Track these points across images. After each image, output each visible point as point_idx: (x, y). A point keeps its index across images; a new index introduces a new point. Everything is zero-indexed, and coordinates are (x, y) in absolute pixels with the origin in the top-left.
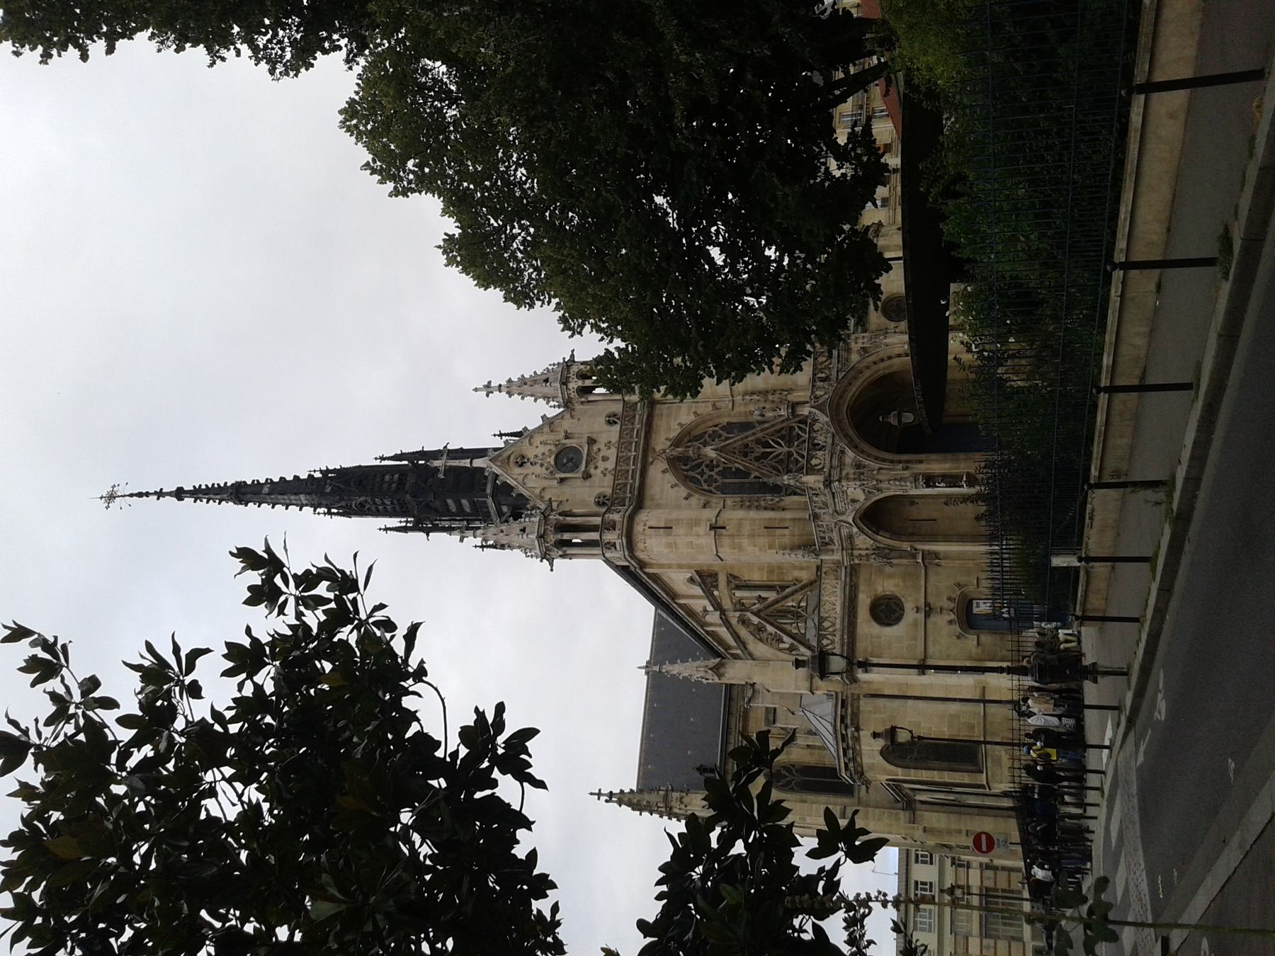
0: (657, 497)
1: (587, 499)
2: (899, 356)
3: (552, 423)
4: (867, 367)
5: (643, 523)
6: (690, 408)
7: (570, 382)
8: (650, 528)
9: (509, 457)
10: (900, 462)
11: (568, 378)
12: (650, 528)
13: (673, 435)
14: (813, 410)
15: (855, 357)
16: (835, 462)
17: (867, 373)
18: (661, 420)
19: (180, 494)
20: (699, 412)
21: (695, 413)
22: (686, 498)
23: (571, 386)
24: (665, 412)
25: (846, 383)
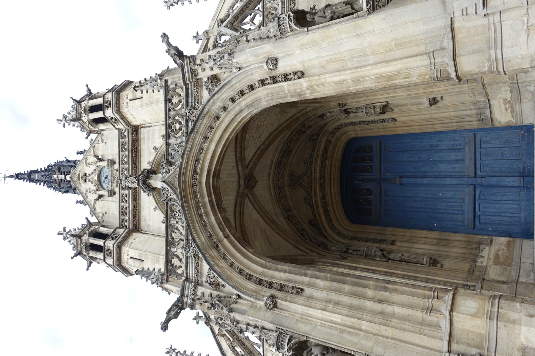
0: (147, 218)
1: (115, 213)
2: (263, 82)
3: (94, 147)
4: (225, 109)
5: (126, 254)
7: (82, 117)
8: (131, 258)
9: (79, 175)
10: (271, 285)
11: (81, 113)
12: (131, 258)
13: (151, 159)
14: (165, 185)
15: (205, 94)
17: (226, 118)
18: (144, 143)
19: (18, 176)
23: (83, 119)
24: (146, 135)
25: (199, 138)
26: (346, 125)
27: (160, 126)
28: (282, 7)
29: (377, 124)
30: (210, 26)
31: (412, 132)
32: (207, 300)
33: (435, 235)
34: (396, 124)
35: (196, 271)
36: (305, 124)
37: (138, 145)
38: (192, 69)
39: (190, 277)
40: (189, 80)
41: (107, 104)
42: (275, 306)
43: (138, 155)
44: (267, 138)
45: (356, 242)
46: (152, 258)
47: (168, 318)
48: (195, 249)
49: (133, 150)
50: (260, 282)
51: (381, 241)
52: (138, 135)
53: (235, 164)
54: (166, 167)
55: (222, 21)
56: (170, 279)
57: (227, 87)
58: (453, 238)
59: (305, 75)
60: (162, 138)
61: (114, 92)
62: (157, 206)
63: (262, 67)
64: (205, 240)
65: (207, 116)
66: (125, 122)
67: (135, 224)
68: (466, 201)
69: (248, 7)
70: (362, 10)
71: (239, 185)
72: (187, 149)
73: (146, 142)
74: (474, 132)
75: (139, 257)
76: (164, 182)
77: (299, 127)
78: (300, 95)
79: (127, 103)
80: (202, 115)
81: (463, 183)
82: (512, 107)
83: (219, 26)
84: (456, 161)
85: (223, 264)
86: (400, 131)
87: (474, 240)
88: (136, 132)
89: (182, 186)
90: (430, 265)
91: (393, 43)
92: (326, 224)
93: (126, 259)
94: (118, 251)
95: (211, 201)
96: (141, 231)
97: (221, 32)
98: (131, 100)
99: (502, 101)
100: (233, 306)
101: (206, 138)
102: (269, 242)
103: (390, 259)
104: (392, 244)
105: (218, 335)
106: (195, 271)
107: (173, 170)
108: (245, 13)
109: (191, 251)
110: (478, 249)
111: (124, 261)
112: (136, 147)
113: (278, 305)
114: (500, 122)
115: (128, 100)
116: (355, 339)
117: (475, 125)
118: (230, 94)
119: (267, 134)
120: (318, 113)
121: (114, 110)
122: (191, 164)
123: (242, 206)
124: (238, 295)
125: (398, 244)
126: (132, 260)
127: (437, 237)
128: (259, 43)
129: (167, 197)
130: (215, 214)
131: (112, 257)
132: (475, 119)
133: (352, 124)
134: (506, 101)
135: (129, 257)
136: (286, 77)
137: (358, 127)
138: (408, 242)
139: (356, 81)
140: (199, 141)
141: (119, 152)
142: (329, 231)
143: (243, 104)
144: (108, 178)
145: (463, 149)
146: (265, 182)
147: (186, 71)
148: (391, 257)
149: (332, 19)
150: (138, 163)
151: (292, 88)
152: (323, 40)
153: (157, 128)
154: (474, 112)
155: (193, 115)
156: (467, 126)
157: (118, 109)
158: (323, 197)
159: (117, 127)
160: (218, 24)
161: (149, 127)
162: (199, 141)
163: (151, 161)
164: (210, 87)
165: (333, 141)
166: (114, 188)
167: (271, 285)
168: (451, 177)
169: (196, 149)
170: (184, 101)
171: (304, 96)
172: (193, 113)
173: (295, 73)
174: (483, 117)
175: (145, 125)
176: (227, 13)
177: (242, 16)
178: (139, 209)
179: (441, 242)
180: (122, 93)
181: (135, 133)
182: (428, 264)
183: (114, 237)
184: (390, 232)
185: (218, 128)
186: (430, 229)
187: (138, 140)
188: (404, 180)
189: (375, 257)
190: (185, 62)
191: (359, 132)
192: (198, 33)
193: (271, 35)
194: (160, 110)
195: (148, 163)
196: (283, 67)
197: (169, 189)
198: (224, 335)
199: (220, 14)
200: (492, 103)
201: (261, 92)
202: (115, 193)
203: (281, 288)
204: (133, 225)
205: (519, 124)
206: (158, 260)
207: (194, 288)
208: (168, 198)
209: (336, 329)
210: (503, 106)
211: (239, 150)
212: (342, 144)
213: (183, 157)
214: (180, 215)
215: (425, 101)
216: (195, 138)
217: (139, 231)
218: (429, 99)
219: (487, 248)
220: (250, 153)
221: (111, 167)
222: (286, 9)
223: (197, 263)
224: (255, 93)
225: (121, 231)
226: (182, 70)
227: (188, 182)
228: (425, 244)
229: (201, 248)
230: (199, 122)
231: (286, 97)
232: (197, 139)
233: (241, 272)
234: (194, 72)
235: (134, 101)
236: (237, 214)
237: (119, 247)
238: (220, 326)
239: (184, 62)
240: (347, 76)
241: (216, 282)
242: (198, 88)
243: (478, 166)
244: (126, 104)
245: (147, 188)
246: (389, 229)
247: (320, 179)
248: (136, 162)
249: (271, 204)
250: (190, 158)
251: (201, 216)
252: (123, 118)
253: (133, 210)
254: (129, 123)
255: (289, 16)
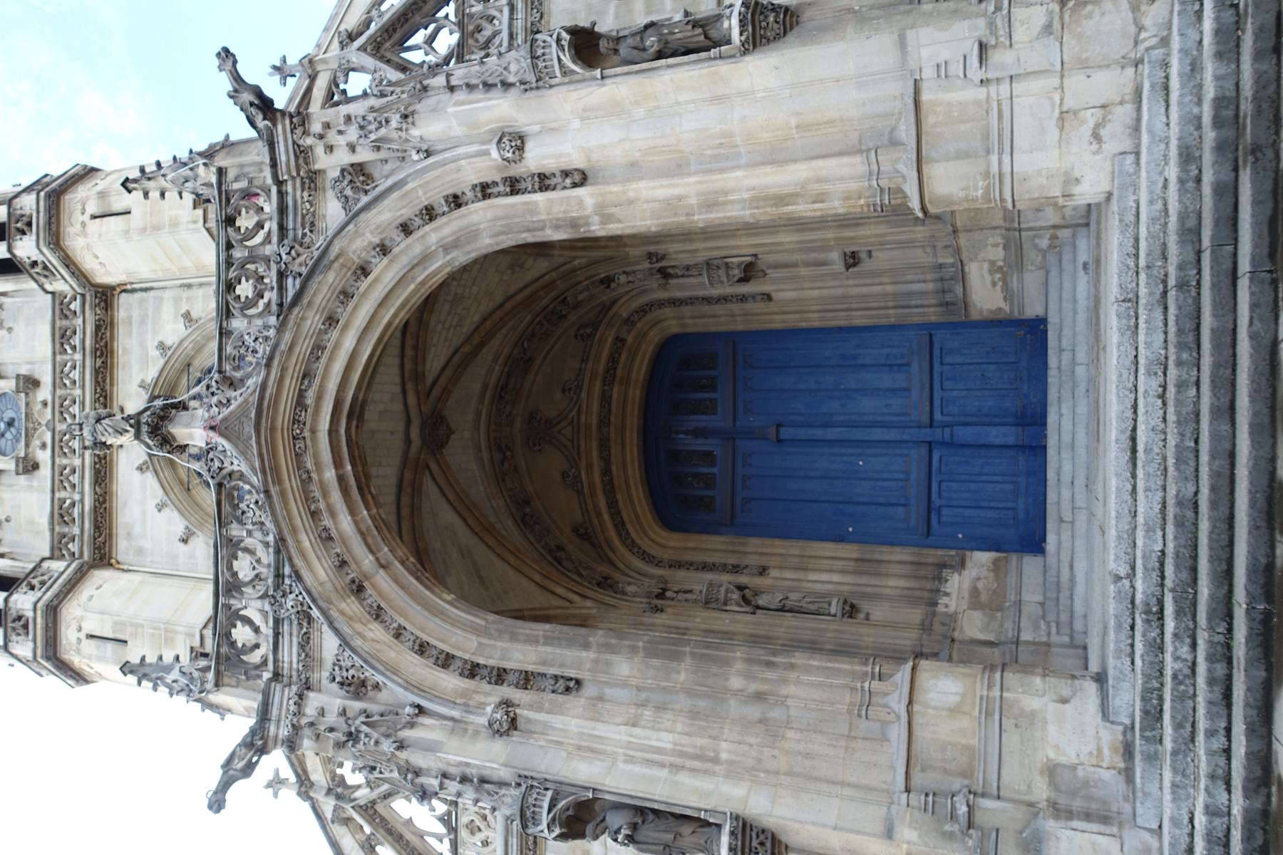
0: (137, 530)
1: (38, 520)
2: (485, 190)
4: (384, 249)
5: (74, 626)
6: (177, 300)
8: (91, 637)
10: (499, 676)
12: (91, 637)
13: (151, 374)
15: (332, 210)
16: (290, 655)
17: (386, 274)
18: (130, 333)
20: (194, 315)
21: (187, 316)
22: (185, 541)
24: (136, 314)
25: (313, 320)
26: (661, 304)
27: (176, 290)
28: (511, 19)
29: (729, 306)
30: (318, 46)
31: (804, 325)
32: (334, 725)
33: (849, 551)
34: (772, 307)
35: (303, 655)
36: (565, 298)
37: (112, 338)
38: (299, 146)
39: (286, 672)
40: (289, 173)
41: (19, 225)
42: (513, 723)
43: (112, 364)
44: (477, 328)
45: (682, 573)
46: (153, 635)
47: (225, 779)
48: (300, 598)
49: (96, 350)
50: (473, 671)
51: (736, 569)
52: (112, 310)
53: (398, 389)
54: (219, 392)
55: (352, 37)
56: (226, 680)
57: (395, 195)
58: (887, 557)
59: (590, 180)
60: (182, 320)
61: (42, 194)
62: (166, 498)
63: (487, 153)
64: (328, 576)
65: (336, 265)
66: (73, 273)
67: (99, 548)
68: (913, 476)
69: (420, 9)
70: (729, 42)
71: (408, 441)
72: (283, 347)
73: (134, 331)
74: (929, 329)
75: (113, 632)
76: (212, 428)
77: (552, 306)
78: (574, 223)
79: (84, 224)
80: (325, 262)
81: (906, 437)
82: (1004, 280)
83: (343, 46)
84: (894, 391)
85: (376, 631)
86: (777, 323)
87: (930, 560)
88: (106, 304)
89: (266, 441)
90: (843, 615)
91: (793, 122)
92: (613, 535)
93: (74, 641)
94: (50, 620)
95: (341, 479)
96: (117, 566)
97: (348, 61)
98: (94, 217)
99: (986, 266)
100: (406, 734)
101: (331, 321)
102: (480, 577)
103: (758, 607)
104: (761, 574)
105: (333, 822)
106: (299, 655)
107: (240, 400)
108: (411, 22)
109: (291, 603)
110: (940, 579)
111: (67, 647)
112: (106, 342)
113: (521, 723)
114: (981, 311)
115: (86, 218)
116: (704, 783)
117: (933, 315)
118: (399, 214)
119: (477, 318)
120: (599, 274)
121: (41, 242)
122: (290, 385)
123: (416, 490)
124: (419, 707)
125: (774, 573)
126: (93, 642)
127: (854, 556)
128: (478, 95)
129: (221, 469)
130: (352, 512)
131: (31, 637)
132: (934, 302)
133: (675, 302)
134: (994, 268)
135: (82, 635)
136: (544, 182)
137: (687, 310)
138: (797, 569)
139: (710, 203)
140: (314, 326)
141: (54, 354)
142: (622, 549)
143: (433, 238)
144: (16, 424)
145: (908, 365)
146: (467, 434)
147: (282, 148)
148: (761, 602)
149: (660, 55)
150: (112, 385)
151: (556, 209)
152: (637, 103)
153: (167, 294)
154: (930, 286)
155: (298, 260)
156: (916, 316)
157: (55, 239)
158: (606, 471)
159: (49, 287)
160: (341, 43)
161: (146, 290)
162: (314, 326)
163: (149, 381)
164: (348, 192)
165: (630, 340)
166: (34, 452)
167: (499, 676)
168: (883, 425)
169: (304, 347)
170: (272, 226)
171: (586, 228)
172: (299, 255)
173: (566, 174)
174: (948, 297)
175: (134, 286)
176: (364, 16)
177: (403, 29)
178: (111, 507)
179: (863, 566)
180: (67, 197)
181: (103, 304)
182: (839, 614)
183: (35, 582)
184: (756, 548)
185: (363, 295)
186: (841, 539)
187: (112, 323)
188: (786, 433)
189: (725, 604)
190: (280, 127)
191: (689, 321)
192: (284, 60)
193: (511, 79)
194: (180, 246)
195: (140, 386)
196: (537, 157)
197: (227, 446)
198: (347, 821)
199: (345, 19)
200: (967, 269)
201: (478, 213)
202: (36, 466)
203: (527, 680)
204: (95, 549)
205: (1016, 315)
206: (172, 639)
207: (296, 698)
208: (224, 472)
209: (662, 765)
210: (988, 279)
211: (409, 352)
212: (651, 349)
213: (268, 365)
214: (258, 513)
215: (835, 256)
216: (303, 318)
217: (111, 565)
218: (845, 253)
219: (956, 575)
220: (435, 362)
221: (27, 394)
222: (520, 25)
223: (306, 633)
224: (464, 216)
225: (58, 565)
226: (269, 145)
227: (282, 430)
228: (830, 571)
229: (316, 595)
230: (317, 278)
231: (543, 229)
232: (309, 322)
233: (422, 649)
234: (302, 154)
235: (105, 219)
236: (405, 512)
237: (53, 611)
238: (339, 797)
239: (275, 125)
240: (688, 188)
241: (359, 678)
242: (313, 193)
243: (937, 402)
244: (79, 226)
245: (161, 444)
246: (754, 544)
247: (599, 427)
248: (104, 381)
249: (482, 488)
250: (287, 369)
251: (315, 515)
252: (69, 262)
253: (95, 509)
254: (85, 277)
255: (559, 40)
